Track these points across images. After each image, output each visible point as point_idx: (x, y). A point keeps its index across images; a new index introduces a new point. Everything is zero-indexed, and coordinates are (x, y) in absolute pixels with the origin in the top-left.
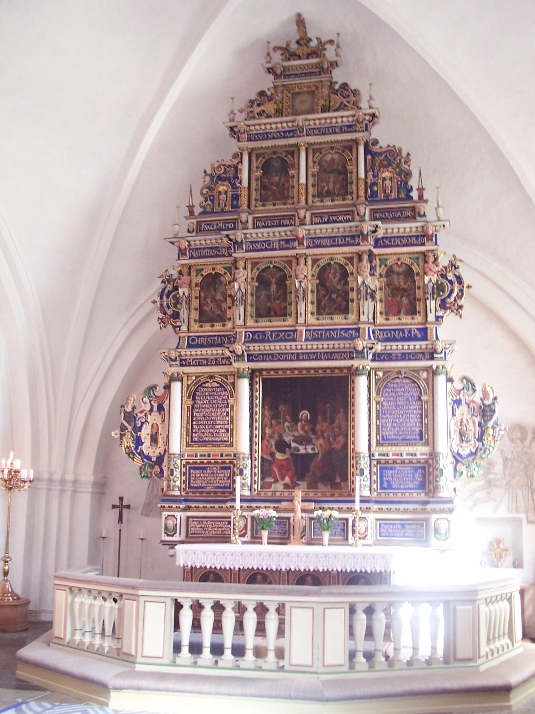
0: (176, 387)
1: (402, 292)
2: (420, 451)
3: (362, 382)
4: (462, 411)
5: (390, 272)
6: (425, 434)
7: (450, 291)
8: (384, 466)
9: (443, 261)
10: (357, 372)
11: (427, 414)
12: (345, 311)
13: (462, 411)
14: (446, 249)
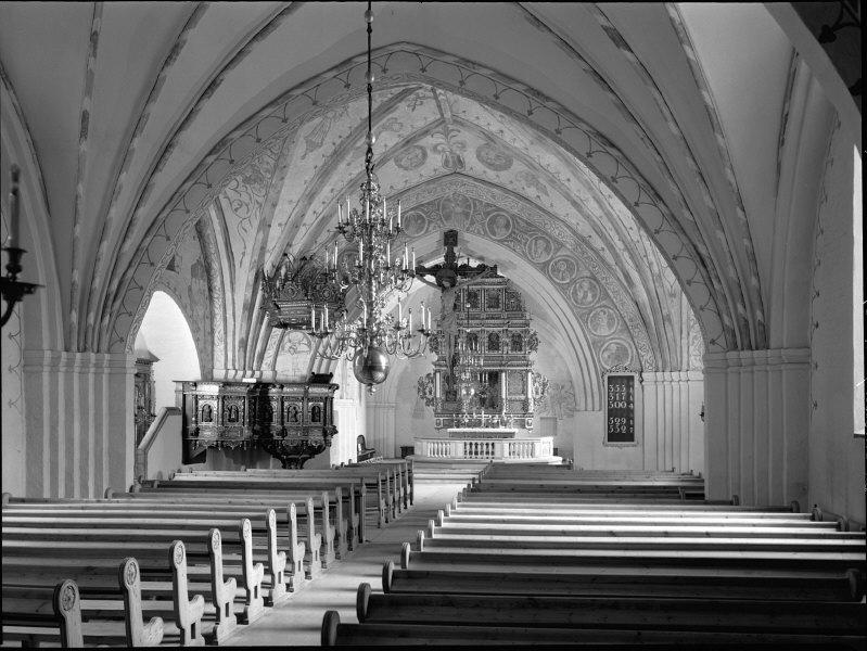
0: (438, 375)
1: (517, 343)
2: (523, 397)
3: (504, 374)
4: (537, 384)
5: (513, 336)
6: (524, 392)
7: (533, 343)
8: (511, 401)
9: (532, 333)
10: (502, 371)
11: (525, 384)
12: (498, 349)
13: (537, 384)
14: (533, 328)
